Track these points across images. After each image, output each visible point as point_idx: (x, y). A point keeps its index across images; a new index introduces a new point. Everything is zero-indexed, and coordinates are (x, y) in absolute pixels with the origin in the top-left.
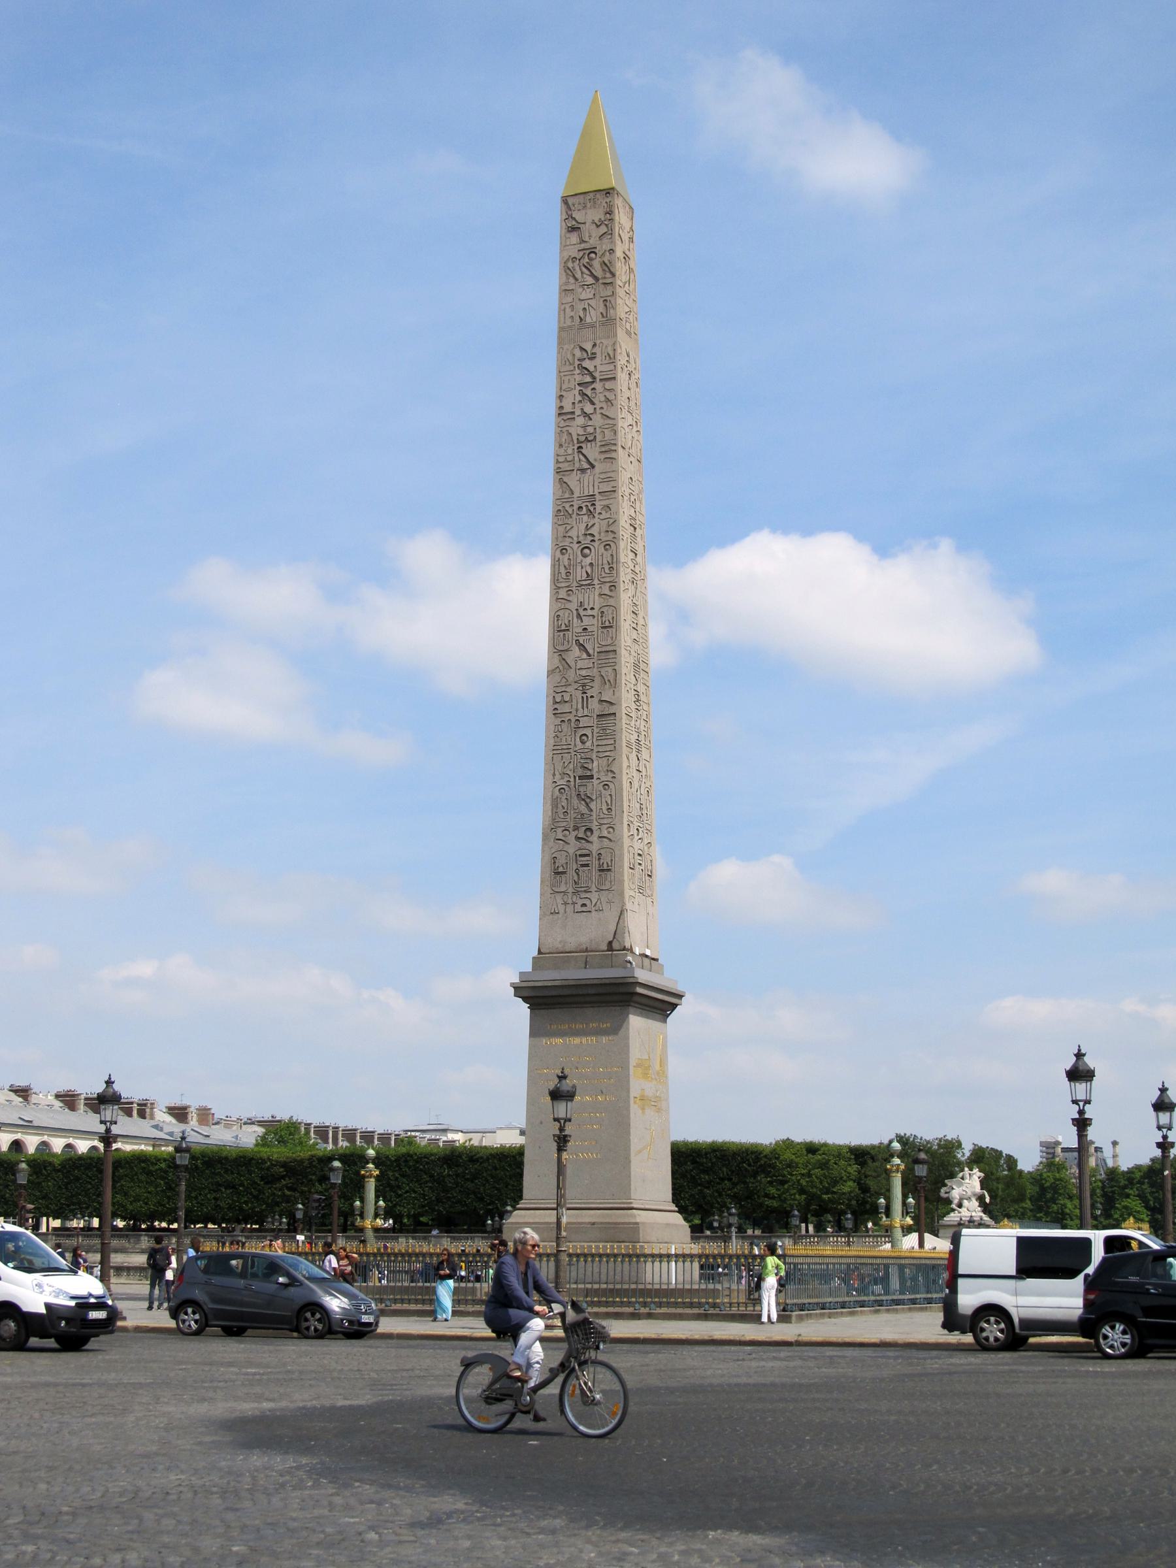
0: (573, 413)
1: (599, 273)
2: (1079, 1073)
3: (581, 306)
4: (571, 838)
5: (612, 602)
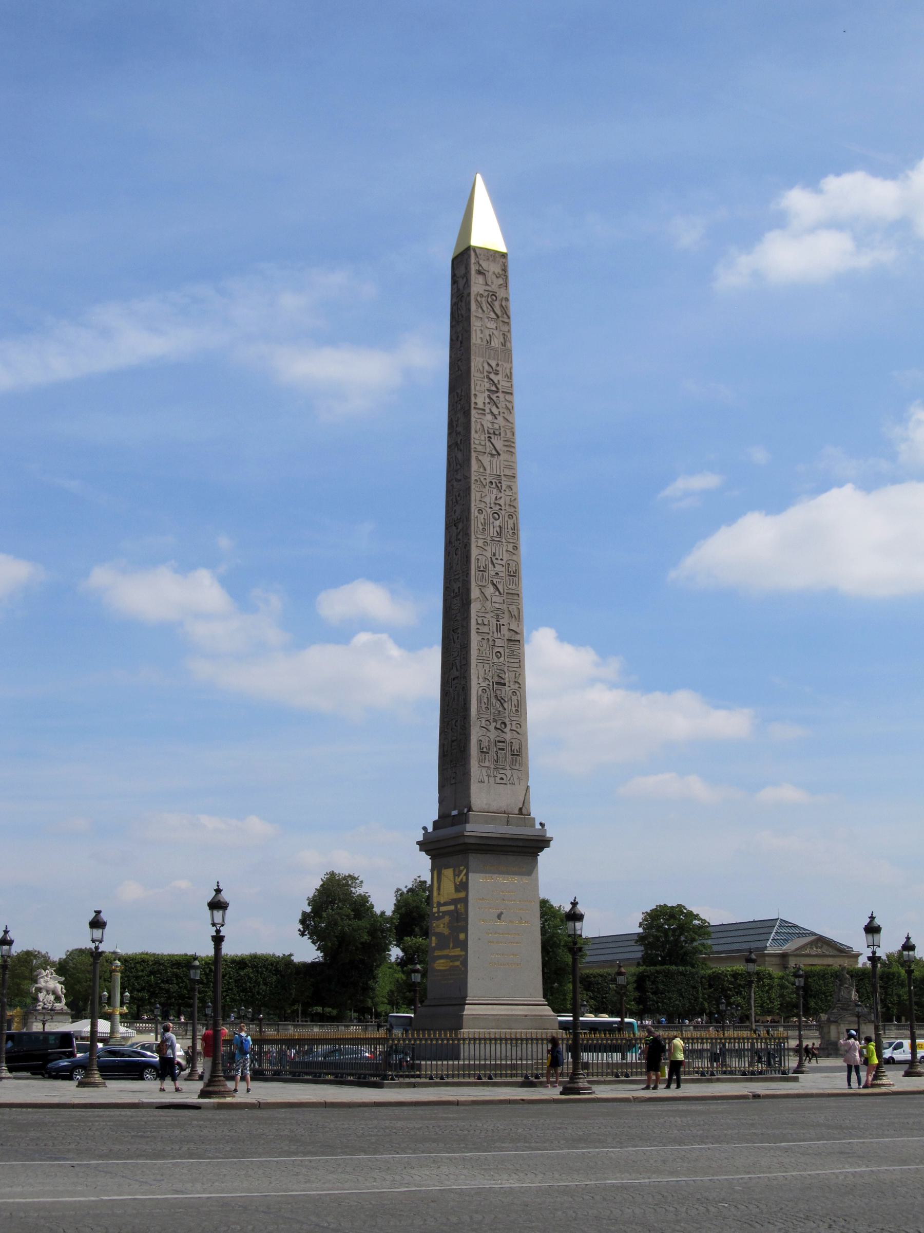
0: (484, 410)
1: (499, 313)
2: (217, 905)
3: (487, 332)
4: (492, 728)
5: (514, 557)
